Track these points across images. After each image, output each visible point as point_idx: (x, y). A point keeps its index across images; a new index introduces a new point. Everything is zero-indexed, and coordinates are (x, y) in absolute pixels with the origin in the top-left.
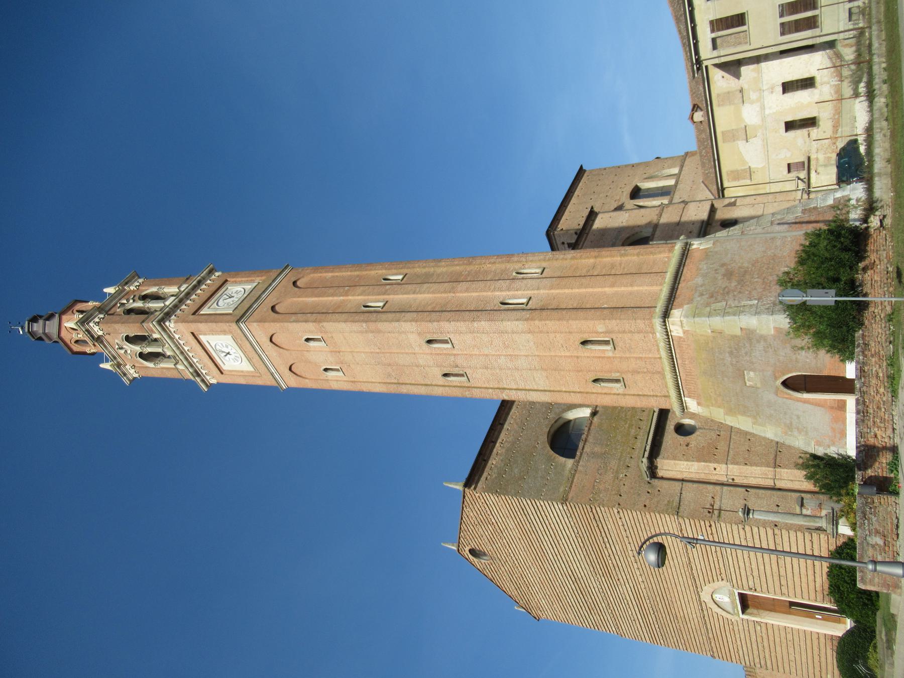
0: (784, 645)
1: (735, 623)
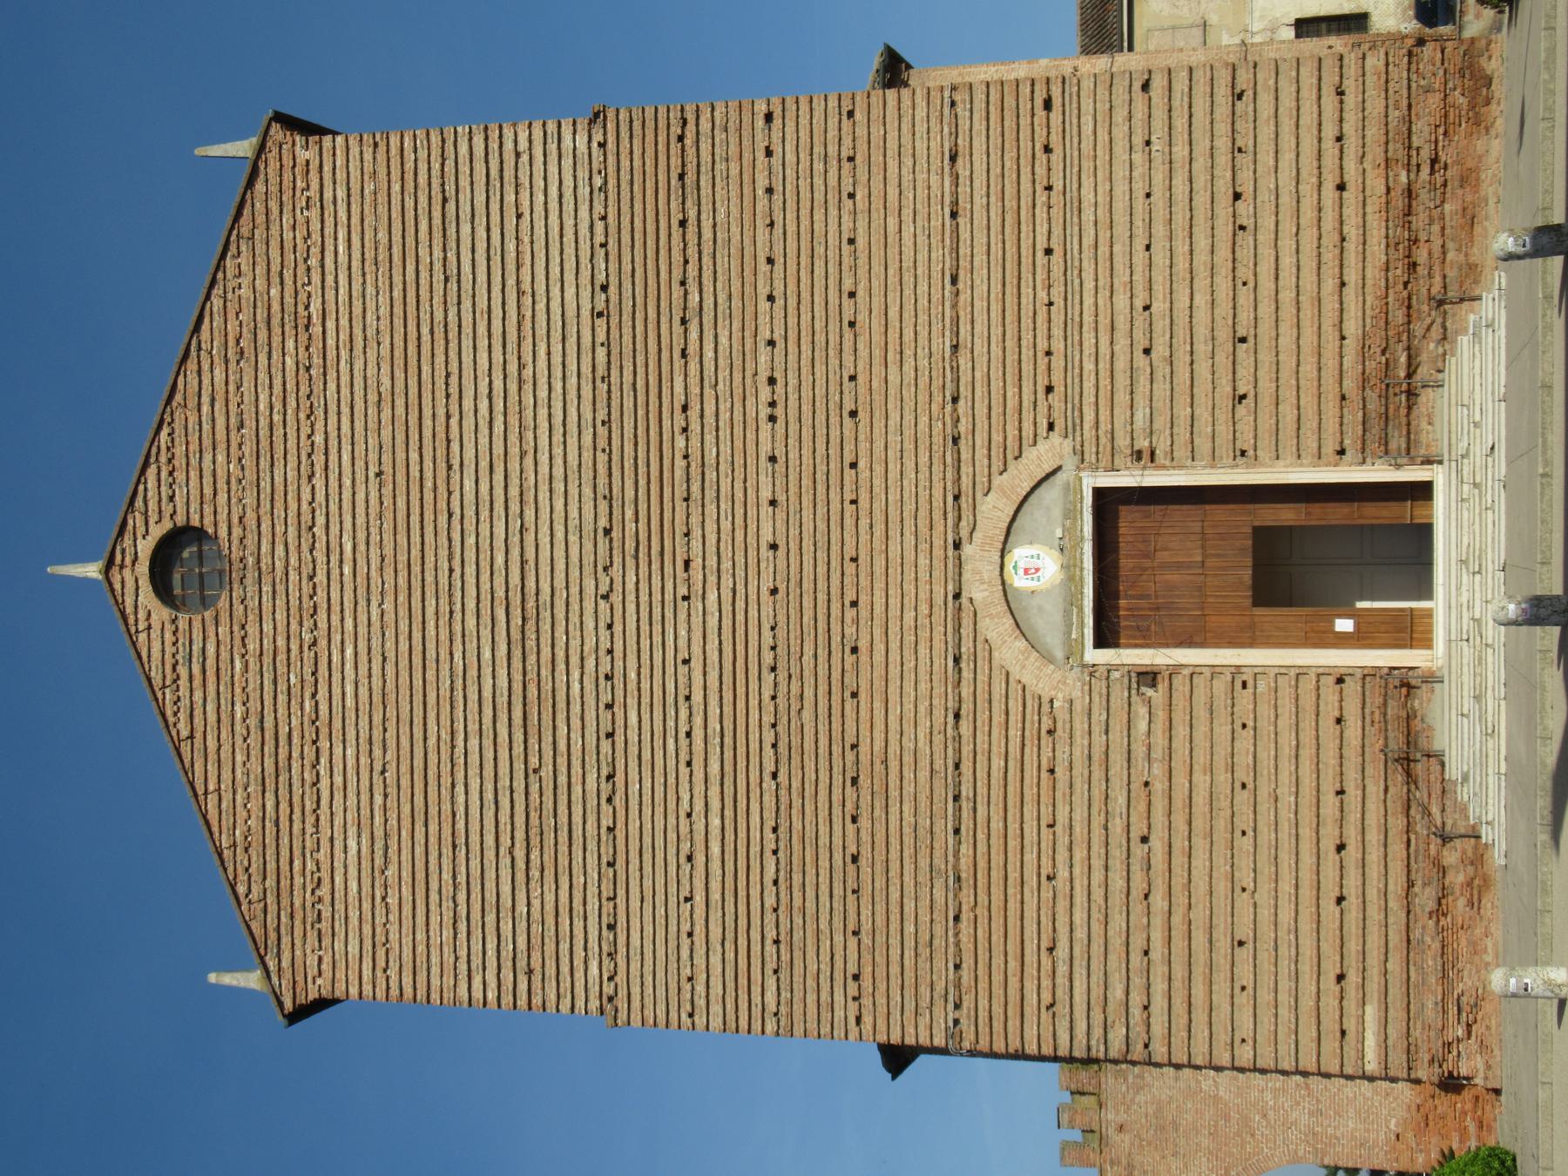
0: (1221, 824)
1: (1062, 716)
